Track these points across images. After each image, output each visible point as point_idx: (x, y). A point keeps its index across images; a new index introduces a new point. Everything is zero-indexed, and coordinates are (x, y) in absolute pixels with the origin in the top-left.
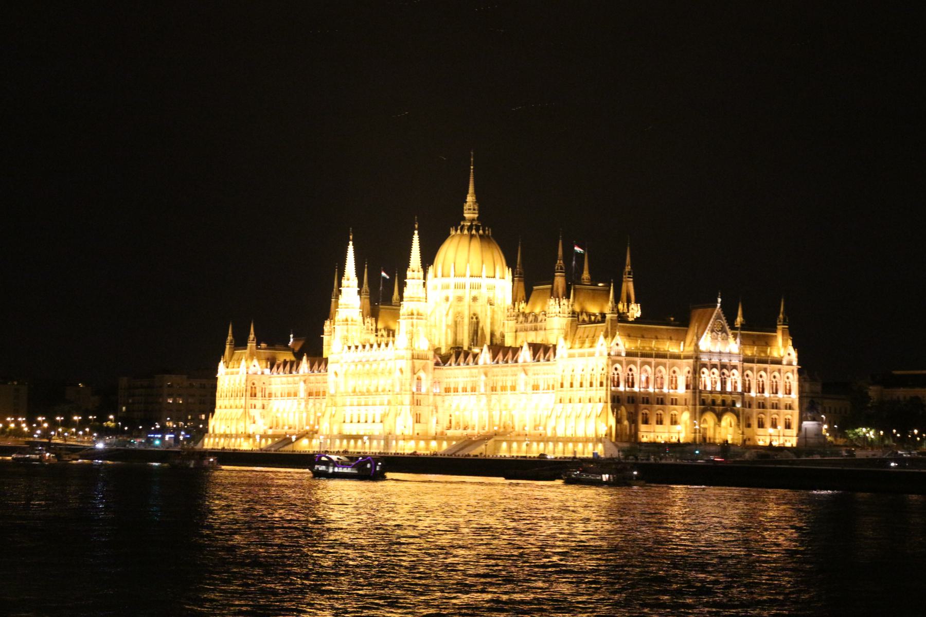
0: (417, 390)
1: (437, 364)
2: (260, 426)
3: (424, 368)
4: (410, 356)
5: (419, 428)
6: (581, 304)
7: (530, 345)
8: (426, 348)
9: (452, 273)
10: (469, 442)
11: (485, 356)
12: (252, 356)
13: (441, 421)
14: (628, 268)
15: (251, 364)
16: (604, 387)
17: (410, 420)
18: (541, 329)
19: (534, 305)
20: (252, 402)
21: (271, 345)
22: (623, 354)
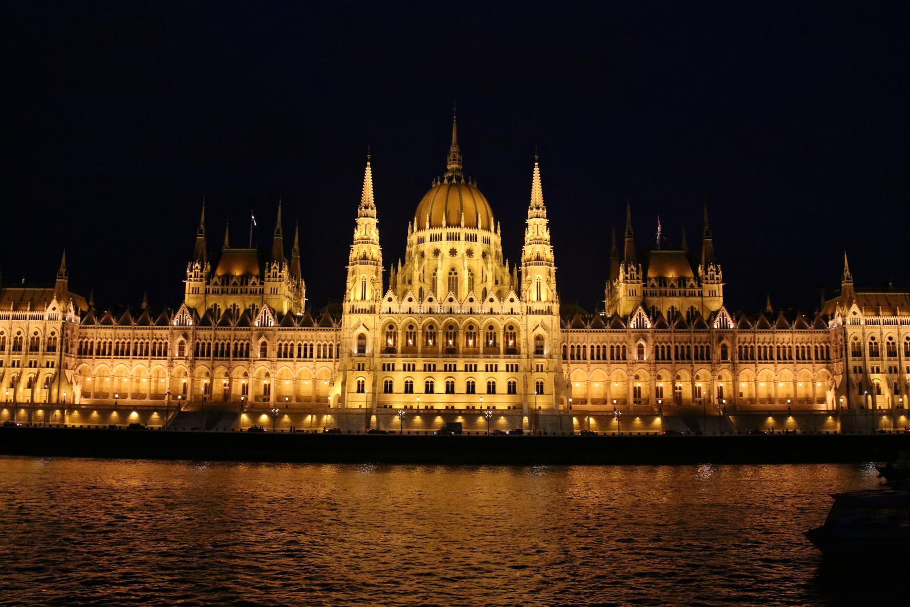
18: (692, 295)
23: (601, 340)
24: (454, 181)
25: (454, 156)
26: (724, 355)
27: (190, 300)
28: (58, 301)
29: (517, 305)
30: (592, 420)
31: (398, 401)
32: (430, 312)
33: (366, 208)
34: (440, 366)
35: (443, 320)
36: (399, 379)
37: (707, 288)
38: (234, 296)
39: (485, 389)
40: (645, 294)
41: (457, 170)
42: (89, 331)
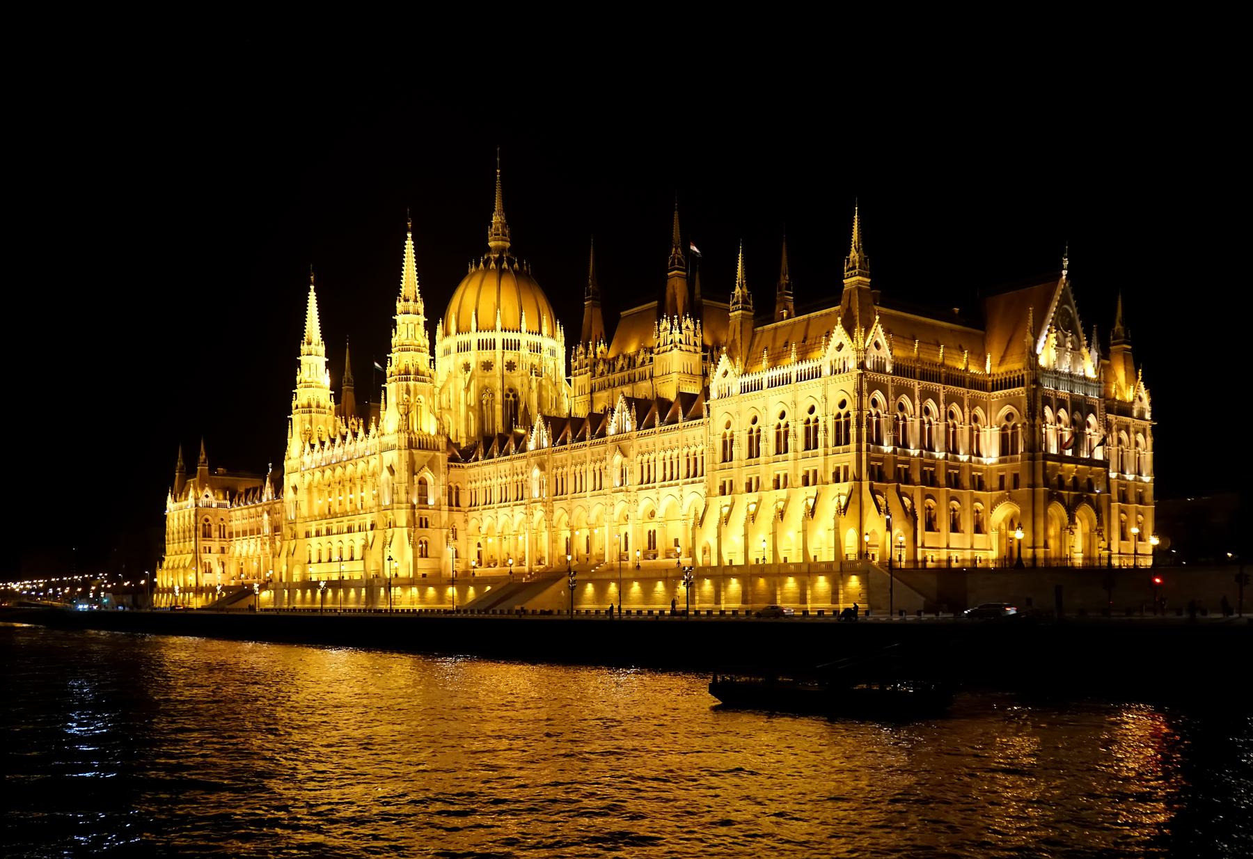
0: (420, 501)
1: (453, 459)
3: (432, 465)
4: (404, 443)
5: (424, 566)
6: (713, 334)
7: (629, 401)
8: (433, 432)
10: (514, 587)
11: (539, 436)
13: (462, 554)
15: (201, 495)
16: (853, 445)
18: (643, 378)
19: (624, 342)
20: (207, 546)
21: (233, 470)
22: (889, 368)
28: (195, 488)
34: (335, 531)
35: (334, 470)
40: (592, 392)
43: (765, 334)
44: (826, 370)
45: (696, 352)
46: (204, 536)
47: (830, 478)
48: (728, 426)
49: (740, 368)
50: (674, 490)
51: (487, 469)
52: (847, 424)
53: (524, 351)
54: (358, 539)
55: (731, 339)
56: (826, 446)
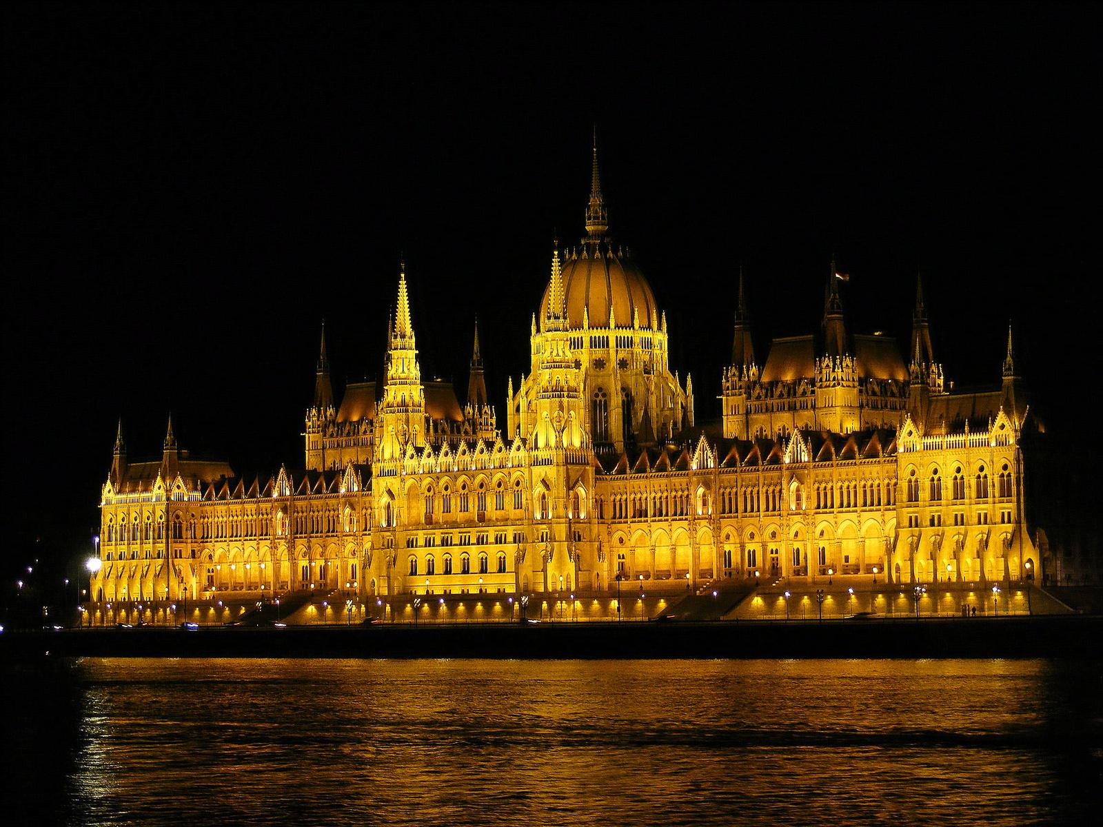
0: (574, 517)
1: (598, 472)
2: (193, 586)
3: (583, 478)
4: (561, 459)
7: (806, 434)
9: (586, 326)
12: (169, 474)
14: (920, 306)
16: (1014, 498)
17: (571, 567)
18: (804, 407)
19: (779, 369)
23: (663, 487)
24: (574, 256)
25: (596, 212)
26: (799, 505)
27: (311, 461)
28: (164, 479)
29: (522, 453)
30: (614, 604)
31: (421, 586)
32: (448, 471)
33: (396, 337)
35: (456, 478)
36: (421, 555)
37: (821, 395)
38: (349, 450)
39: (495, 569)
40: (748, 413)
41: (596, 235)
42: (209, 509)
43: (939, 404)
44: (993, 444)
45: (854, 387)
46: (175, 537)
47: (999, 519)
48: (913, 473)
49: (921, 432)
50: (853, 516)
51: (636, 483)
52: (1009, 482)
53: (638, 349)
54: (493, 552)
55: (912, 405)
56: (994, 497)
